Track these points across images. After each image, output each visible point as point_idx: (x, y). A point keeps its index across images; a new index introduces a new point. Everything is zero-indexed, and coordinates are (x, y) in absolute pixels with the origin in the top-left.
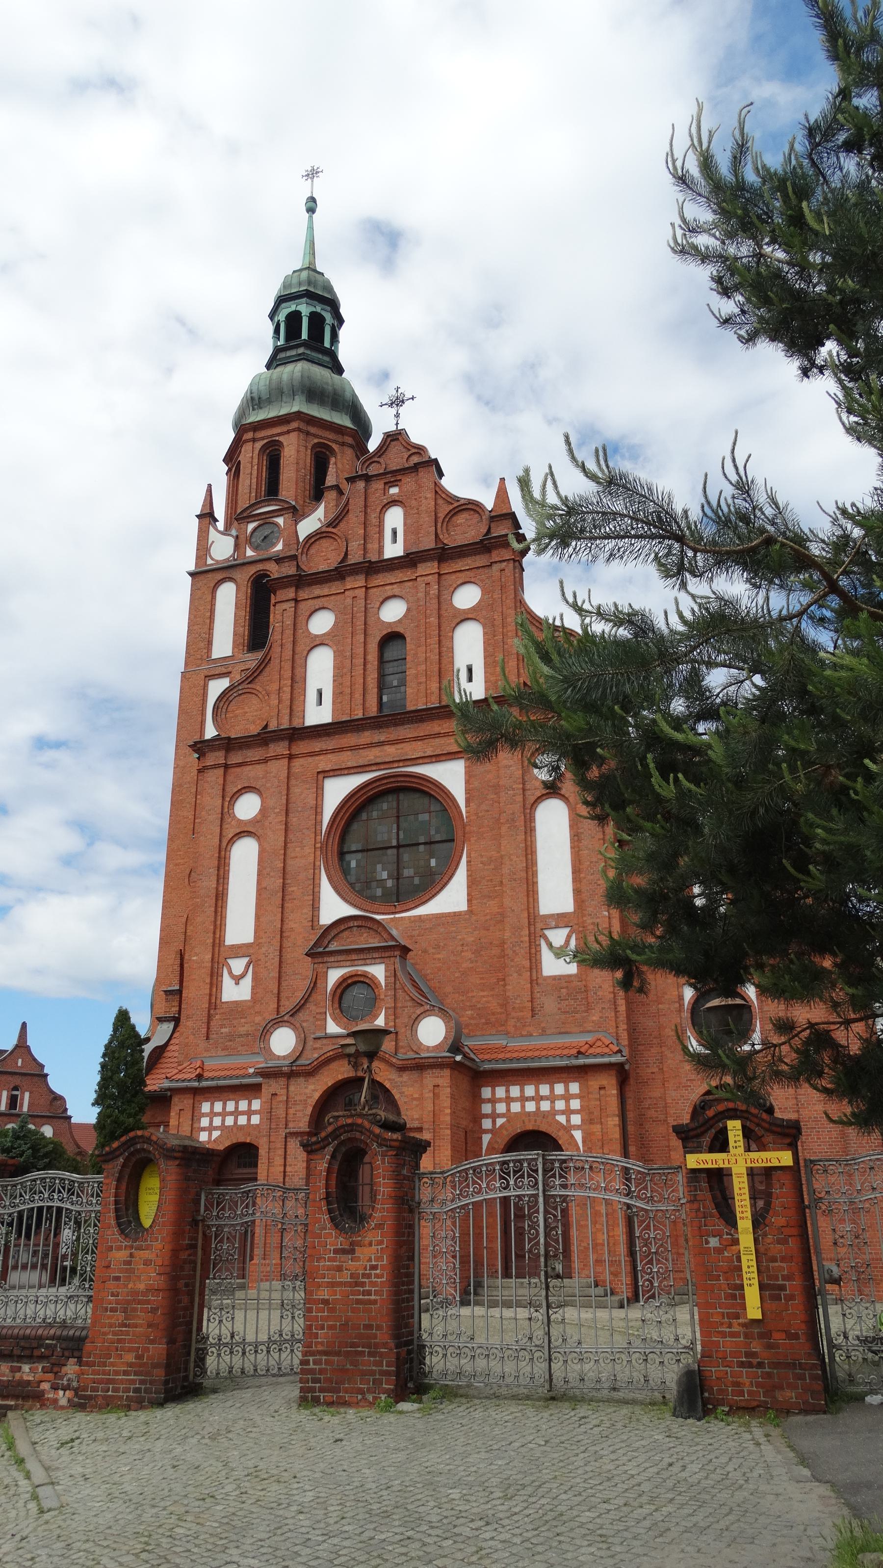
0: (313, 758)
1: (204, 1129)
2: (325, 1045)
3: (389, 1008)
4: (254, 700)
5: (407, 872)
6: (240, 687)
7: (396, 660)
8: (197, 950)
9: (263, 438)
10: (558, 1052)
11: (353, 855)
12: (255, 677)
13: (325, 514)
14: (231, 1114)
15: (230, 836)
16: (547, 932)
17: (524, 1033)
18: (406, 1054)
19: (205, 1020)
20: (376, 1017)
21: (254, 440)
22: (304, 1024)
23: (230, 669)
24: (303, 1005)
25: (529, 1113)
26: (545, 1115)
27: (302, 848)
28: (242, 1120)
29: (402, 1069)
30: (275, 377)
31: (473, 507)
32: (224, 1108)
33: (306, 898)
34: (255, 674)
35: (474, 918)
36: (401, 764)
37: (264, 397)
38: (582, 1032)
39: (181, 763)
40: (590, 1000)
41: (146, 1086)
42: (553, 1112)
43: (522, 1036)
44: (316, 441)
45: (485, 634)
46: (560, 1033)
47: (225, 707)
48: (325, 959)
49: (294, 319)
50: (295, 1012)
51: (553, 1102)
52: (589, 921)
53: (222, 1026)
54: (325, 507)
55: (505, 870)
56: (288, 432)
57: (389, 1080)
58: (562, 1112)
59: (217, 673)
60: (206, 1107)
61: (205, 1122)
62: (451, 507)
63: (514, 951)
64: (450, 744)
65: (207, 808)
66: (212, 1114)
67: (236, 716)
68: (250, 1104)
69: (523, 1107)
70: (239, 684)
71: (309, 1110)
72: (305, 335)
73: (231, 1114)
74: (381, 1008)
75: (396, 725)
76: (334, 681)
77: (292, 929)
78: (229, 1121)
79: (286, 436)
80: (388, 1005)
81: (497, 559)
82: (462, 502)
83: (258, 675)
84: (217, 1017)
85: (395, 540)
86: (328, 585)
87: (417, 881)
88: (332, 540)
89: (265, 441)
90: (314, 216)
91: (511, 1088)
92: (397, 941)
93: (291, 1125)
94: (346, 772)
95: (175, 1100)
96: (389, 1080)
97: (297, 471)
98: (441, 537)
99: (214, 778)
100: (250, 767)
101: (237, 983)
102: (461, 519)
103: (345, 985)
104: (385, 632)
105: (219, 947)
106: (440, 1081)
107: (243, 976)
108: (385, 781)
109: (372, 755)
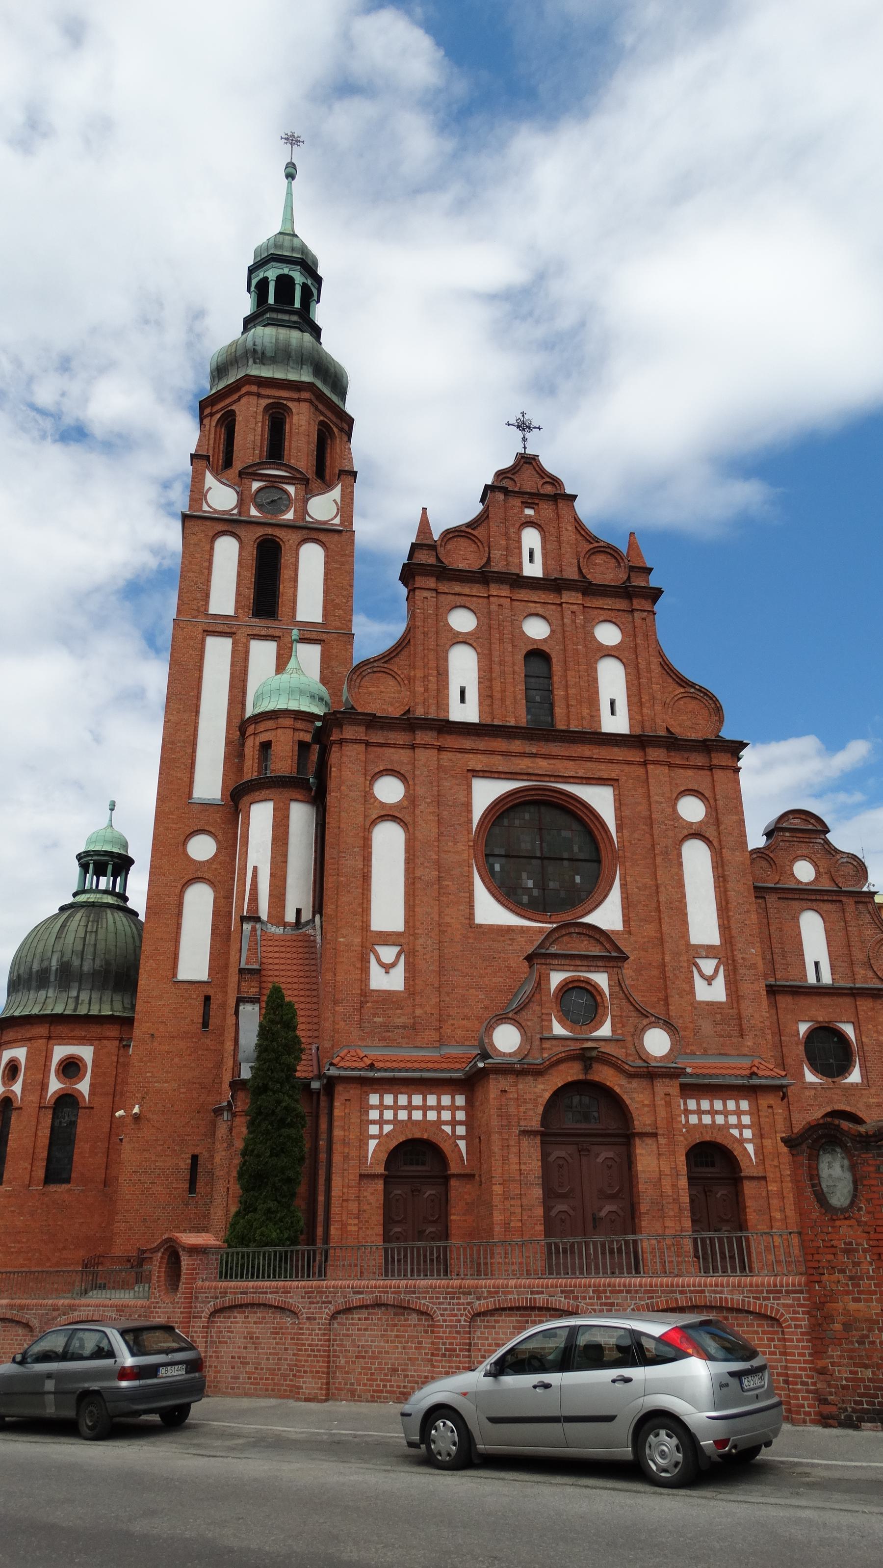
0: (462, 755)
1: (374, 1122)
2: (555, 1046)
3: (616, 1016)
4: (391, 682)
5: (552, 885)
6: (375, 664)
7: (538, 677)
8: (344, 931)
9: (269, 397)
10: (732, 1072)
11: (497, 859)
12: (391, 658)
13: (342, 497)
14: (404, 1108)
15: (374, 816)
16: (698, 960)
17: (688, 1051)
18: (633, 1061)
19: (357, 1006)
20: (601, 1024)
21: (259, 395)
22: (529, 1023)
23: (234, 630)
24: (527, 1003)
25: (706, 1125)
26: (721, 1128)
27: (455, 843)
28: (417, 1115)
29: (631, 1076)
30: (281, 337)
31: (612, 552)
32: (396, 1101)
33: (462, 894)
34: (392, 655)
35: (632, 939)
36: (552, 779)
37: (269, 353)
38: (738, 1055)
39: (173, 719)
40: (744, 1027)
41: (296, 1071)
42: (727, 1126)
43: (686, 1054)
44: (322, 418)
45: (627, 674)
46: (720, 1054)
47: (358, 681)
48: (549, 961)
49: (285, 284)
50: (519, 1010)
51: (726, 1117)
52: (740, 956)
53: (375, 1015)
54: (342, 490)
55: (662, 898)
56: (299, 400)
57: (620, 1086)
58: (735, 1126)
59: (218, 630)
60: (374, 1099)
61: (374, 1115)
62: (592, 546)
63: (675, 974)
64: (600, 770)
65: (348, 783)
66: (382, 1107)
67: (370, 693)
68: (425, 1100)
69: (700, 1119)
70: (375, 661)
71: (540, 1109)
72: (297, 304)
73: (404, 1108)
74: (605, 1015)
75: (547, 740)
76: (479, 683)
77: (448, 925)
78: (403, 1115)
79: (296, 403)
80: (614, 1013)
81: (638, 607)
82: (602, 544)
83: (394, 657)
84: (369, 1005)
85: (531, 560)
86: (469, 585)
87: (563, 894)
88: (470, 541)
89: (271, 401)
90: (293, 182)
91: (689, 1101)
92: (622, 952)
93: (522, 1123)
94: (496, 776)
95: (339, 1089)
96: (620, 1086)
97: (308, 443)
98: (584, 571)
99: (354, 753)
100: (392, 750)
101: (387, 972)
102: (599, 559)
103: (566, 988)
104: (530, 648)
105: (367, 931)
106: (671, 1091)
107: (393, 965)
108: (533, 793)
109: (524, 764)
